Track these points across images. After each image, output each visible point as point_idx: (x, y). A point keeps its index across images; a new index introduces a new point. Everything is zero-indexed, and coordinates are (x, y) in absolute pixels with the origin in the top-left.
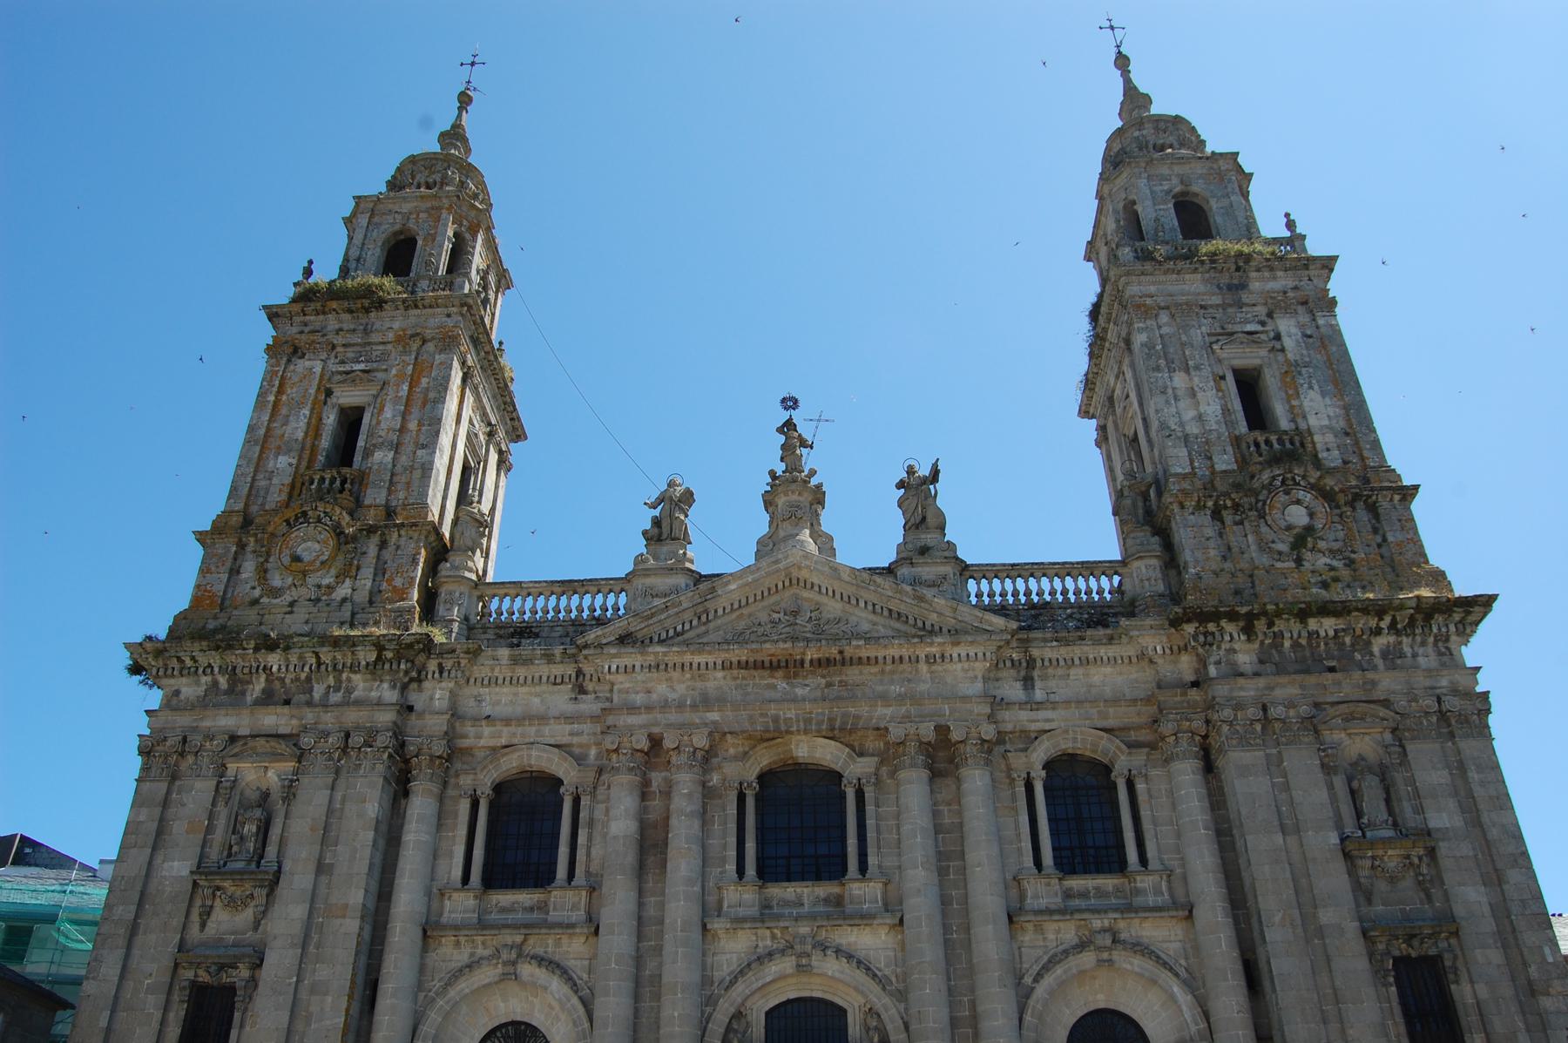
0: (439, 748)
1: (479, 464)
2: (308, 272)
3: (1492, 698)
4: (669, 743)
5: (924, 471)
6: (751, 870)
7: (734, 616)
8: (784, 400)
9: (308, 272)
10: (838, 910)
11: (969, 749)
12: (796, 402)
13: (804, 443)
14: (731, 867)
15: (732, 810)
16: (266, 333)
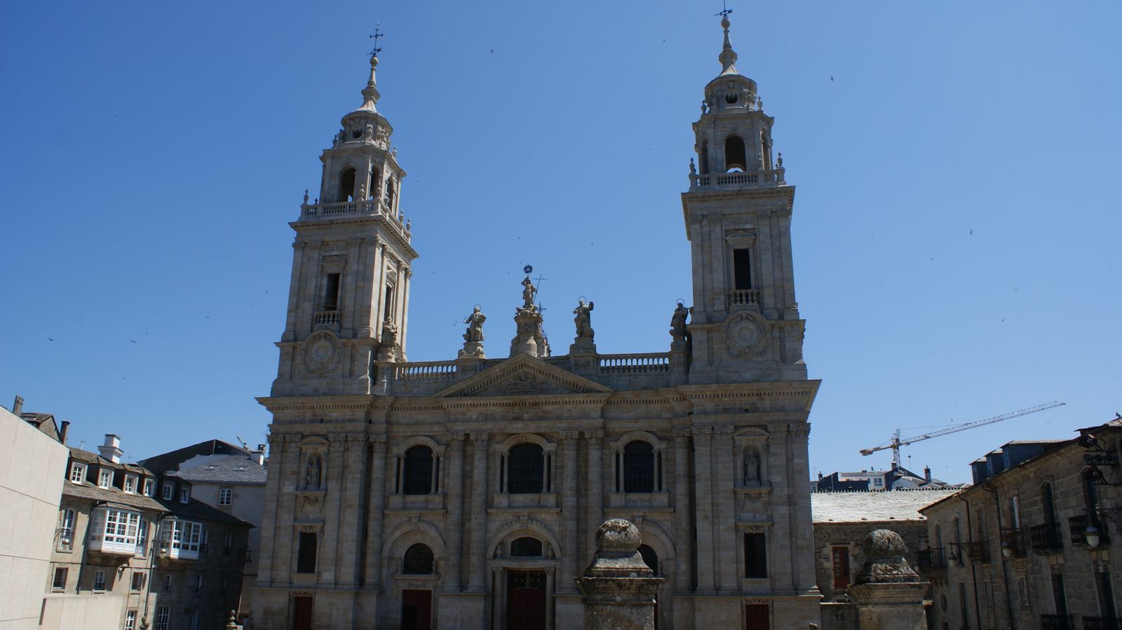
0: (383, 438)
1: (394, 284)
2: (306, 198)
3: (811, 426)
4: (472, 437)
5: (586, 306)
6: (505, 488)
7: (499, 381)
8: (525, 268)
9: (306, 198)
10: (539, 506)
11: (593, 441)
12: (531, 268)
13: (533, 290)
14: (498, 488)
15: (498, 463)
16: (292, 234)
